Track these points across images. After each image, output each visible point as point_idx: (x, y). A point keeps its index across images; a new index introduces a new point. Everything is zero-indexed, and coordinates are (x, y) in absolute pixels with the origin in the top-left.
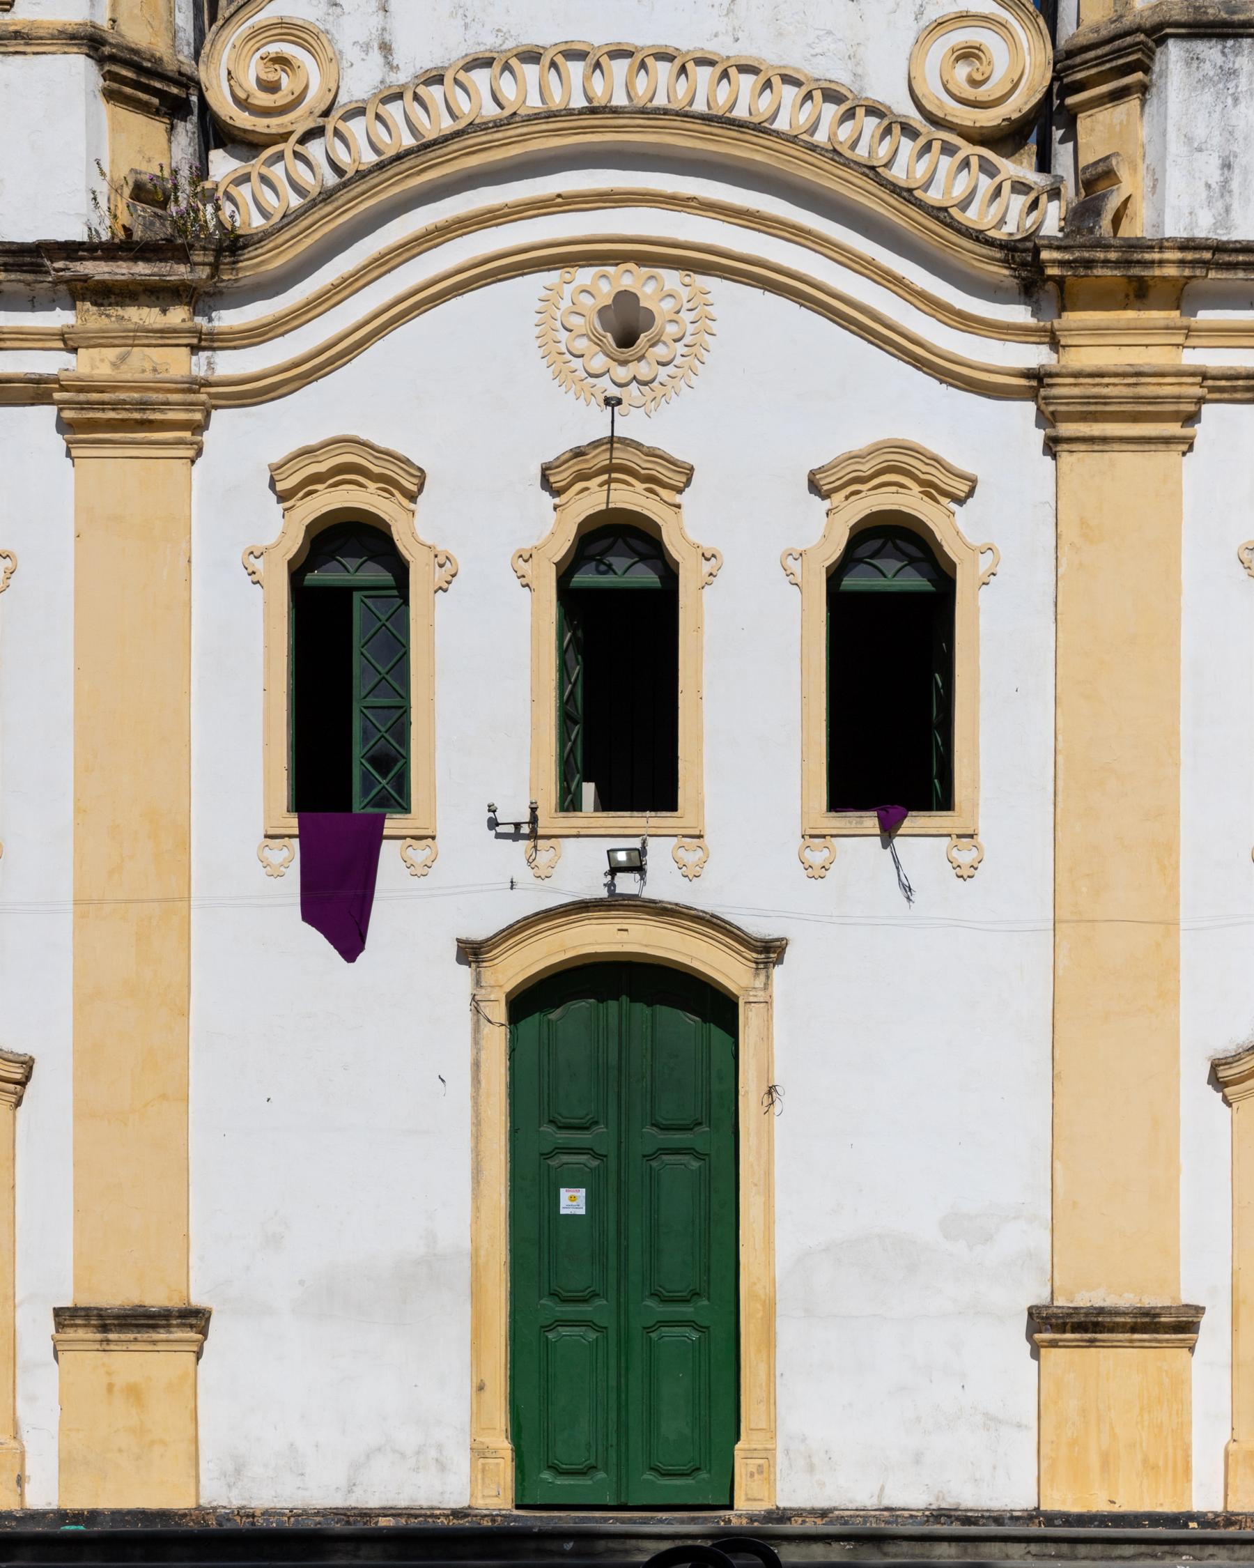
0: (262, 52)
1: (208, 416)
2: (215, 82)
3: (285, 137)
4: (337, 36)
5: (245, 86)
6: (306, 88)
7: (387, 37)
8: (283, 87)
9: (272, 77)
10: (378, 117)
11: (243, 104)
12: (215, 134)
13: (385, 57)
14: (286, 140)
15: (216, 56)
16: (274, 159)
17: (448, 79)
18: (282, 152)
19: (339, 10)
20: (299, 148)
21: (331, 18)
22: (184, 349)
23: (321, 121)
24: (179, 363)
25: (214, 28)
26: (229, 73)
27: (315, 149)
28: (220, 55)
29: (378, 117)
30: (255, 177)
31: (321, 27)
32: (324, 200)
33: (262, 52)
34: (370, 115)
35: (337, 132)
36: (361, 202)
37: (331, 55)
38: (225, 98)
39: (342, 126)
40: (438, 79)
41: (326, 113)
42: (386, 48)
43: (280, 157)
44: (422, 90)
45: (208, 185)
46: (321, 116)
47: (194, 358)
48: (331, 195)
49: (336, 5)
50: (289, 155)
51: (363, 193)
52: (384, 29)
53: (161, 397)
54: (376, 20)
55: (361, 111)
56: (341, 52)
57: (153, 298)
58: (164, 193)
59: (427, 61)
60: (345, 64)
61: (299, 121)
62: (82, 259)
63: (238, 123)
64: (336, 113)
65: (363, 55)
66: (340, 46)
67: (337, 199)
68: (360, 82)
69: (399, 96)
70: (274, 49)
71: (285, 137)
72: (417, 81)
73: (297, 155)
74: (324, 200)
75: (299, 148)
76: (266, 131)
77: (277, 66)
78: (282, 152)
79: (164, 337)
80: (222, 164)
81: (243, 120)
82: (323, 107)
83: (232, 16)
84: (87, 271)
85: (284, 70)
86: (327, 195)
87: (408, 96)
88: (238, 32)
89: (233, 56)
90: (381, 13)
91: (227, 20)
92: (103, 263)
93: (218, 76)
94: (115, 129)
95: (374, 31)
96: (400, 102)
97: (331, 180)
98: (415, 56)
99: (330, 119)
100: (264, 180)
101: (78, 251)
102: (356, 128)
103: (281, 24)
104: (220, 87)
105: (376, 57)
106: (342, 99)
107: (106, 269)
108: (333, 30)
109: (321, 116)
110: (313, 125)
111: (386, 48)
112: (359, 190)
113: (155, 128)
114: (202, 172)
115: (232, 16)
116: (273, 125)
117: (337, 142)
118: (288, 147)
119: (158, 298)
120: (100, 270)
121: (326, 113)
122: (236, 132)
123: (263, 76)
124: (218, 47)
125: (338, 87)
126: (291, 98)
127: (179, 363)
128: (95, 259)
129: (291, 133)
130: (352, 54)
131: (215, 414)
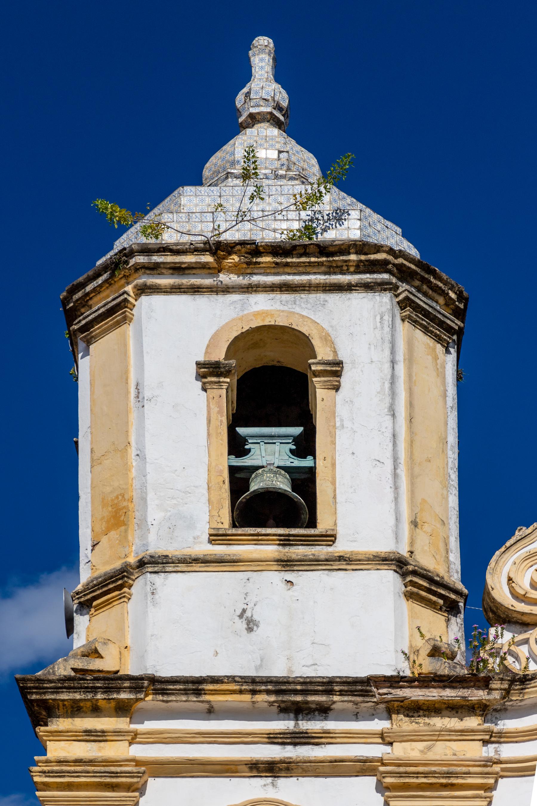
1: (496, 782)
22: (478, 742)
24: (475, 751)
47: (485, 748)
53: (464, 769)
57: (454, 712)
62: (401, 687)
79: (463, 735)
84: (405, 695)
92: (418, 690)
101: (399, 682)
107: (421, 693)
119: (457, 712)
120: (415, 694)
127: (475, 751)
128: (412, 687)
131: (500, 780)
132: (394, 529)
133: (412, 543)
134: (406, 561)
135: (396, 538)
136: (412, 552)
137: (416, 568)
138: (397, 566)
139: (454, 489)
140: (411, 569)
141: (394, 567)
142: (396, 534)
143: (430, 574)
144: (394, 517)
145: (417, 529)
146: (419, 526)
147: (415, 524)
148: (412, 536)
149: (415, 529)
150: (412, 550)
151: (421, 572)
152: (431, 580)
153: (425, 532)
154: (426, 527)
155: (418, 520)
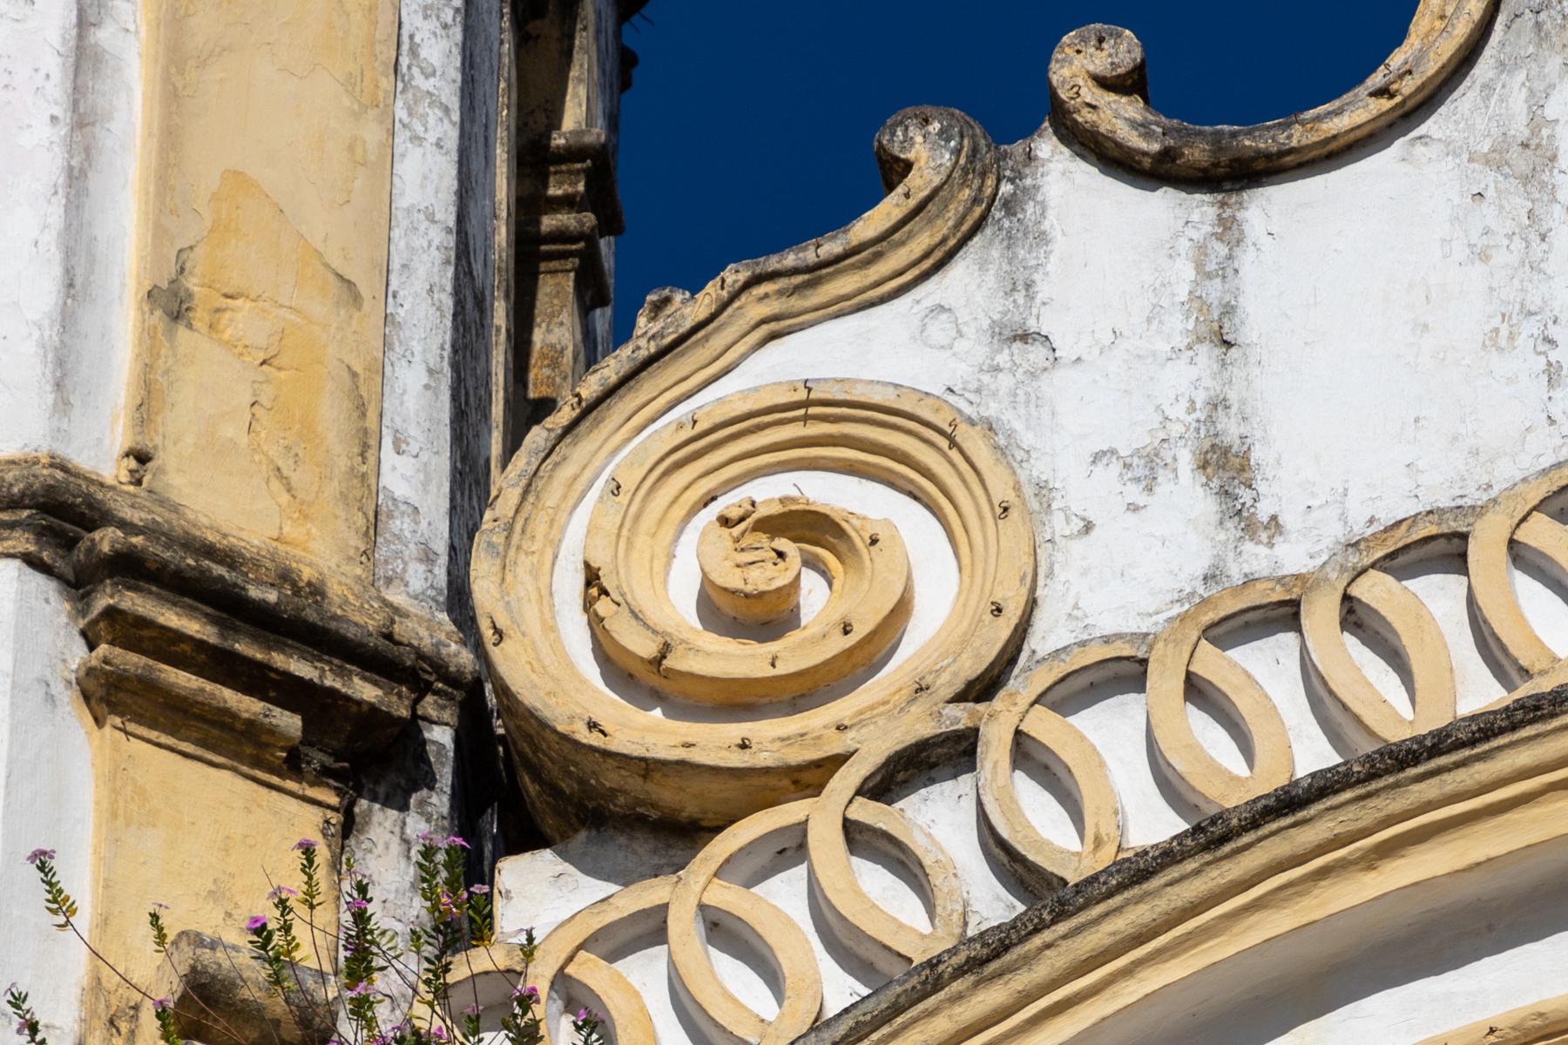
0: (728, 503)
2: (531, 616)
3: (808, 778)
4: (1027, 439)
5: (653, 615)
6: (901, 610)
7: (1231, 429)
8: (806, 616)
9: (767, 577)
10: (1196, 690)
11: (641, 678)
12: (520, 789)
13: (1225, 493)
14: (816, 789)
15: (540, 526)
16: (765, 856)
17: (1486, 550)
18: (802, 828)
19: (1036, 354)
20: (868, 812)
21: (1005, 381)
23: (960, 716)
25: (537, 437)
26: (592, 577)
27: (937, 818)
28: (557, 527)
29: (1196, 690)
30: (684, 925)
31: (968, 410)
32: (973, 965)
33: (728, 503)
34: (1165, 681)
35: (1025, 753)
36: (1127, 972)
37: (1001, 491)
38: (570, 665)
39: (1044, 726)
40: (1443, 550)
41: (984, 688)
42: (1226, 466)
43: (791, 848)
44: (1376, 590)
45: (481, 960)
46: (959, 698)
48: (1005, 948)
49: (1024, 337)
50: (826, 839)
51: (1139, 939)
52: (1218, 404)
54: (1188, 378)
55: (1123, 674)
56: (1042, 488)
58: (304, 1022)
59: (1395, 495)
60: (1058, 525)
61: (873, 719)
63: (621, 742)
64: (1024, 685)
65: (1134, 493)
66: (1039, 468)
67: (1027, 961)
68: (1125, 570)
69: (1284, 615)
70: (769, 492)
71: (808, 778)
72: (1354, 560)
73: (857, 837)
74: (973, 965)
75: (868, 812)
76: (737, 760)
77: (783, 544)
78: (802, 828)
80: (542, 896)
81: (644, 731)
82: (972, 666)
83: (610, 393)
85: (811, 563)
86: (988, 953)
87: (1321, 615)
88: (624, 447)
89: (611, 521)
90: (1207, 354)
91: (590, 409)
93: (547, 595)
94: (115, 780)
95: (1178, 411)
96: (1288, 639)
97: (993, 905)
98: (1334, 479)
99: (999, 702)
100: (723, 931)
102: (1109, 736)
103: (806, 405)
104: (551, 628)
105: (1187, 497)
106: (1047, 637)
108: (1013, 420)
109: (959, 698)
110: (926, 729)
111: (1226, 466)
112: (1121, 924)
113: (290, 818)
114: (462, 924)
115: (610, 393)
116: (772, 740)
117: (1027, 791)
118: (822, 816)
121: (984, 688)
122: (612, 778)
123: (731, 579)
124: (552, 493)
125: (1032, 604)
126: (840, 643)
129: (837, 762)
130: (1084, 489)
132: (52, 334)
133: (146, 407)
134: (91, 503)
135: (58, 386)
136: (143, 458)
137: (137, 540)
138: (41, 533)
139: (434, 114)
140: (106, 548)
141: (23, 542)
142: (60, 363)
143: (219, 570)
144: (57, 271)
145: (182, 331)
146: (200, 316)
147: (171, 304)
148: (148, 367)
149: (171, 335)
150: (147, 443)
151: (164, 565)
152: (228, 605)
153: (230, 345)
154: (243, 322)
155: (192, 283)
